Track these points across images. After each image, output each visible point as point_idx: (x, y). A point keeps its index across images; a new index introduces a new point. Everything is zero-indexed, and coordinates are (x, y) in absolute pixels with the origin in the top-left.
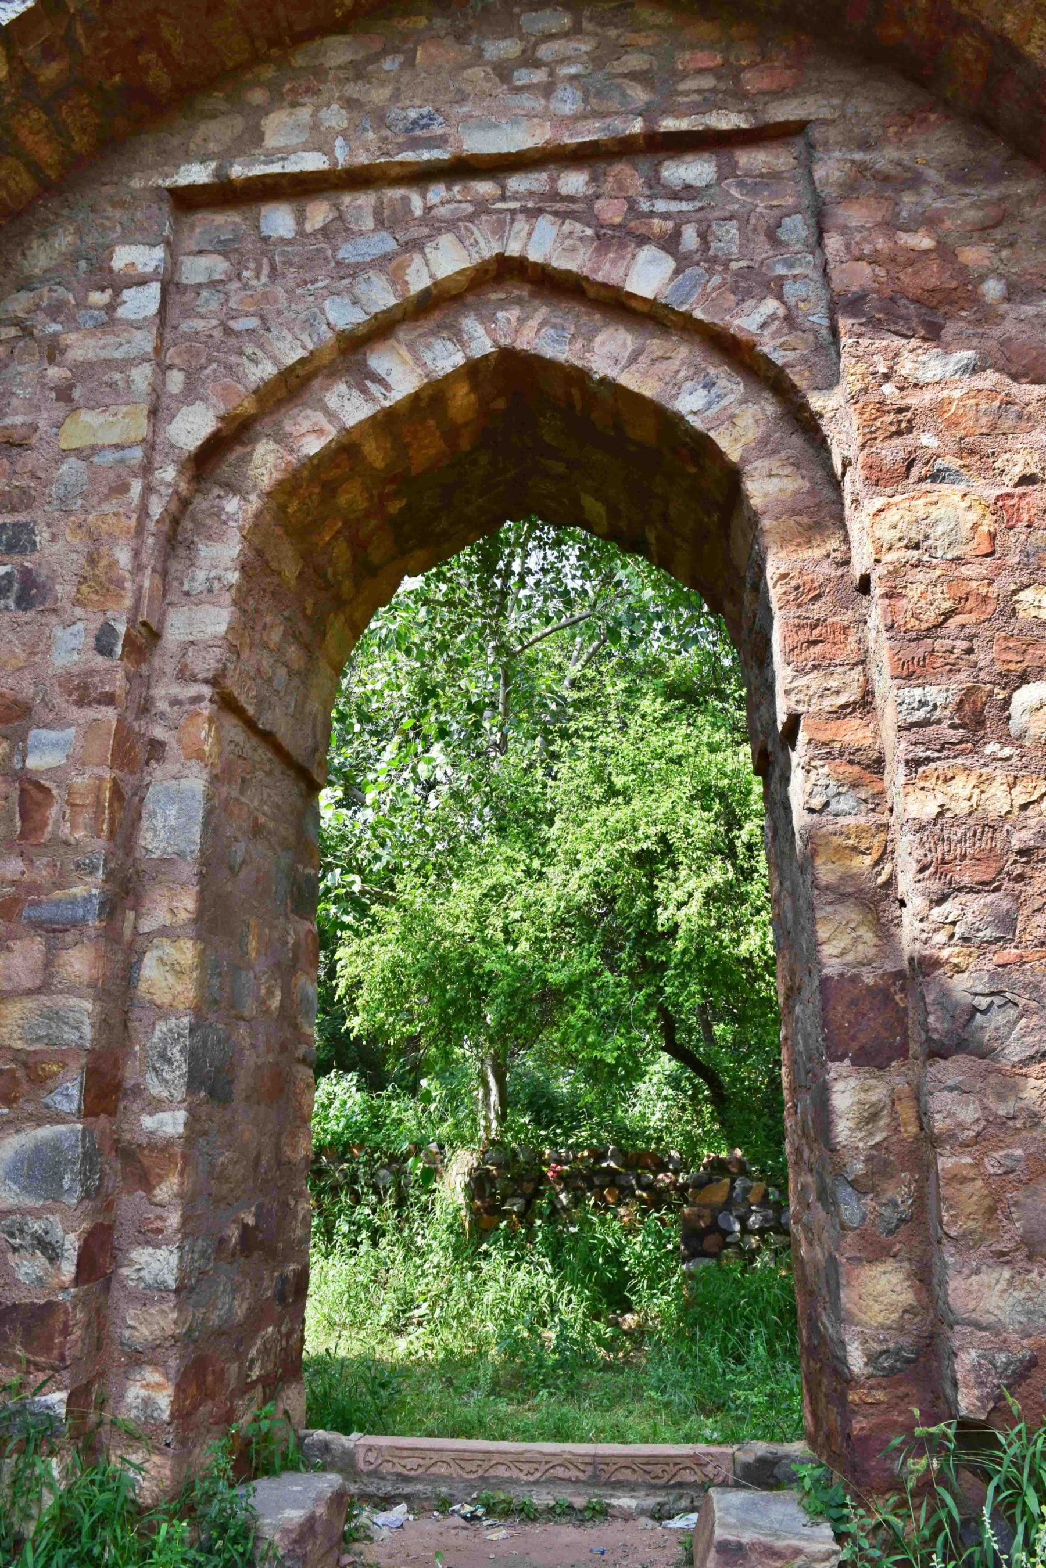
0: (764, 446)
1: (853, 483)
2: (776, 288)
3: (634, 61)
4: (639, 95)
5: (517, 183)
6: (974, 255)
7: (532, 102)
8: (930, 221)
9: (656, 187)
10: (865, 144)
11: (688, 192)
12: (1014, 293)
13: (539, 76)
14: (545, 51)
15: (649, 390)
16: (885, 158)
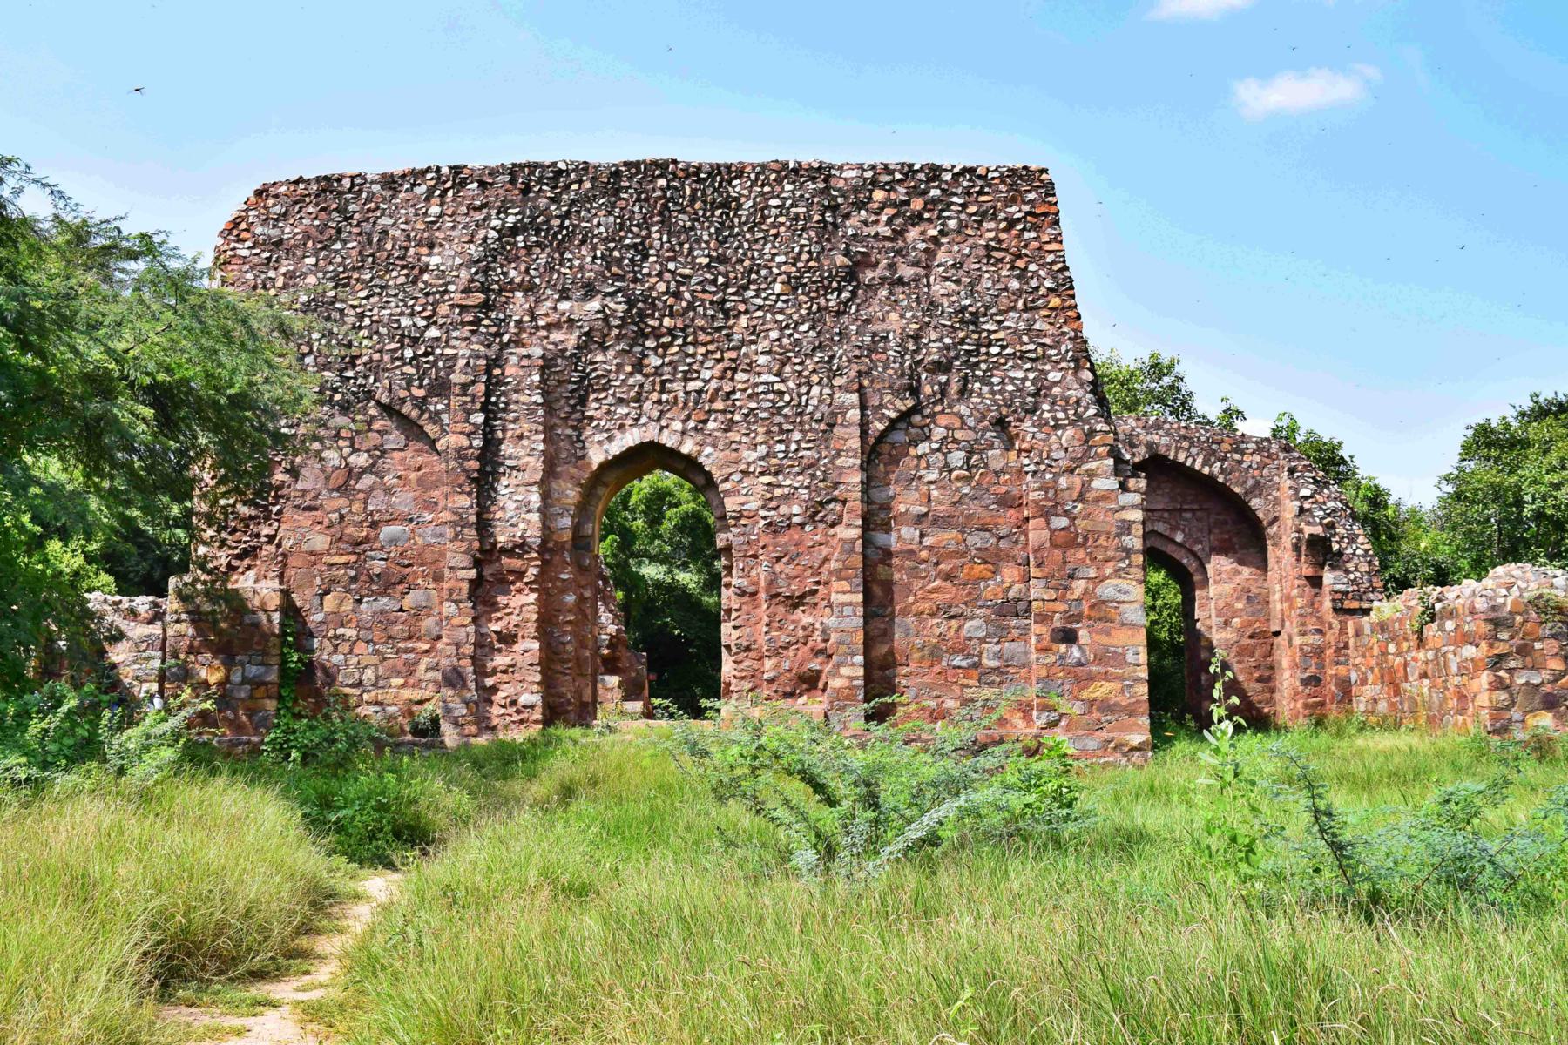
0: (1197, 570)
1: (1211, 581)
2: (1201, 542)
3: (1178, 490)
4: (1179, 499)
5: (1156, 514)
6: (1235, 540)
7: (1159, 498)
8: (1228, 532)
9: (1181, 516)
10: (1218, 514)
11: (1186, 520)
12: (1243, 547)
13: (1160, 492)
14: (1163, 485)
15: (1178, 558)
16: (1221, 517)
